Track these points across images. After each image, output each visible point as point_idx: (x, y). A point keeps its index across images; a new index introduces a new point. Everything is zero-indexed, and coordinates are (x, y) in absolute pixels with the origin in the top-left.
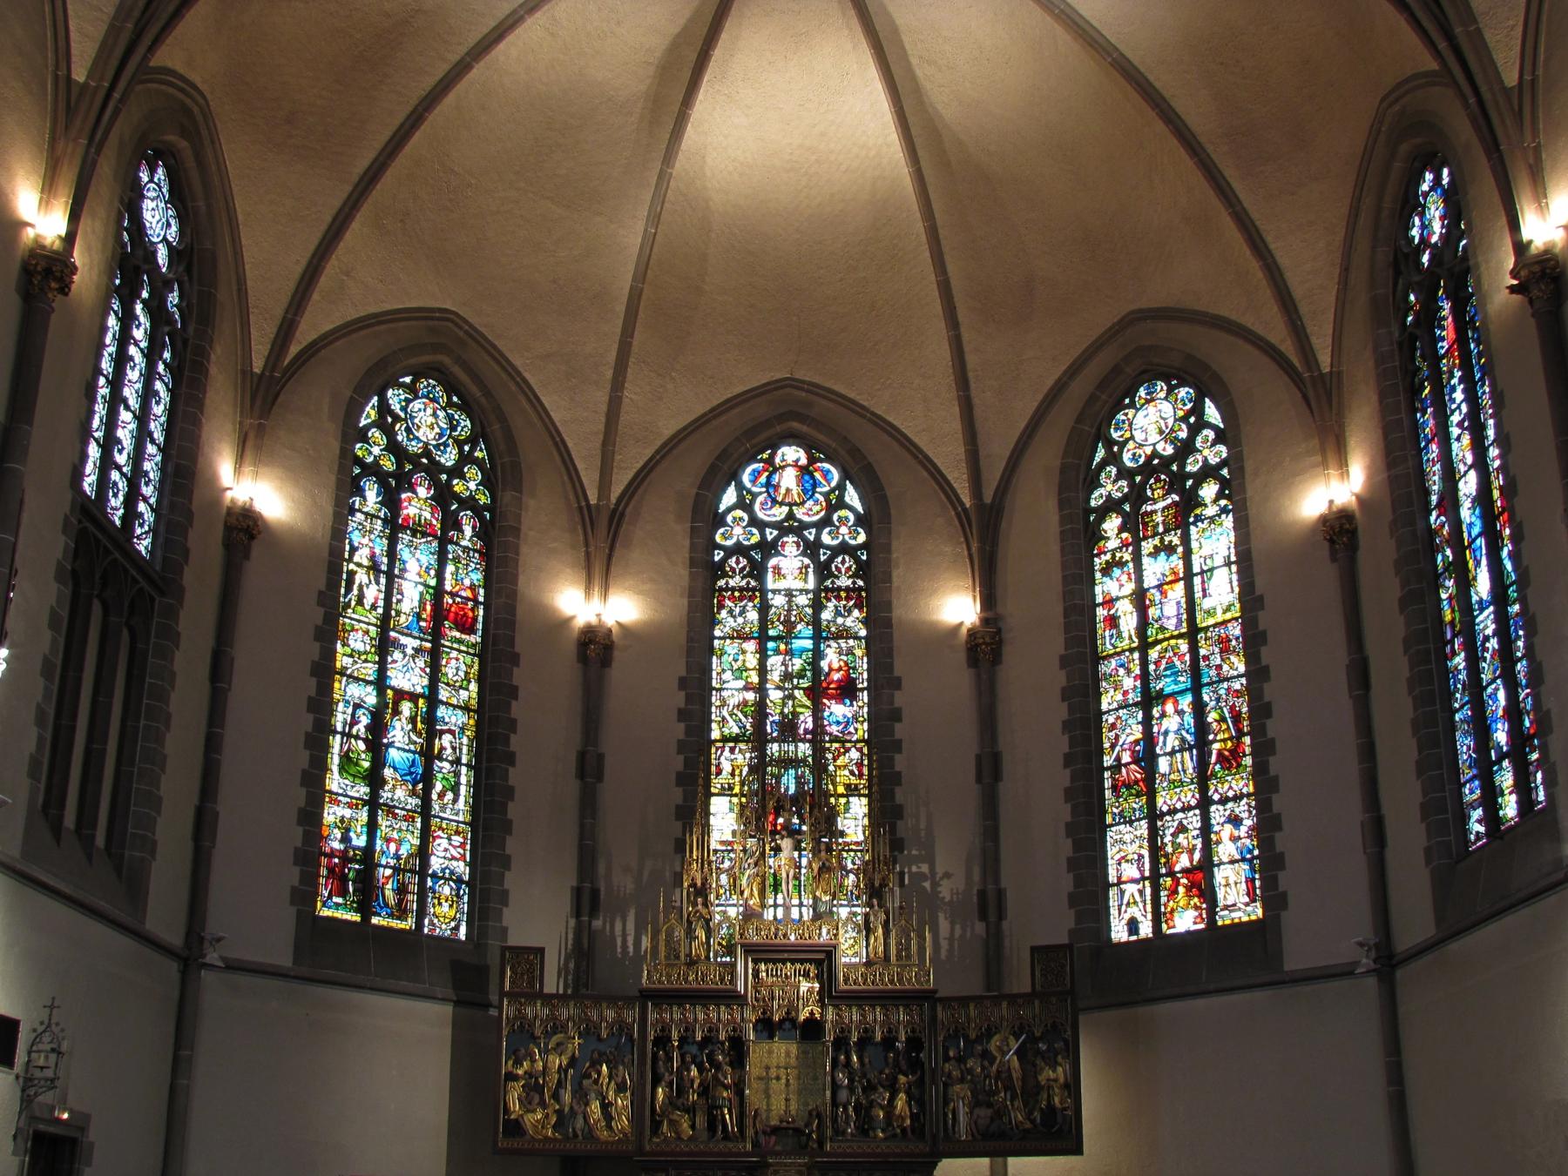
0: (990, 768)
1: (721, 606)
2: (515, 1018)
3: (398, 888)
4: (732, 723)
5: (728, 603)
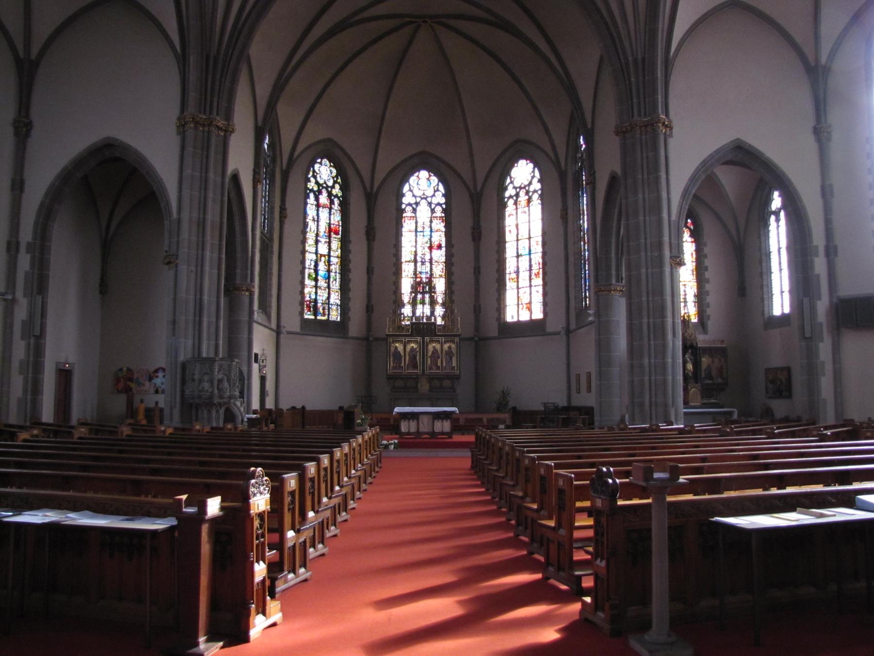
1: (405, 222)
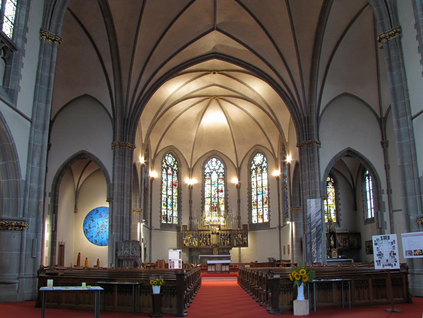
0: (239, 201)
1: (206, 180)
5: (207, 180)
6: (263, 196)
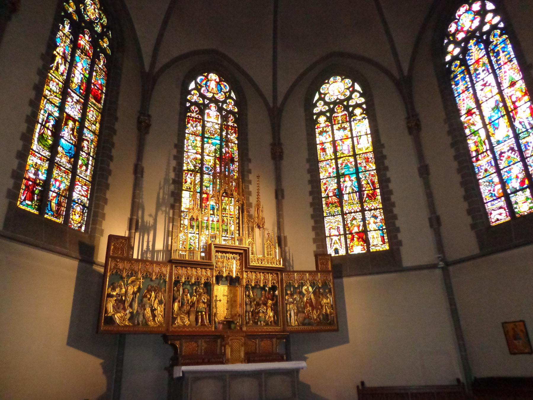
1: (188, 123)
2: (114, 268)
3: (58, 203)
4: (191, 165)
5: (191, 121)
6: (359, 180)
